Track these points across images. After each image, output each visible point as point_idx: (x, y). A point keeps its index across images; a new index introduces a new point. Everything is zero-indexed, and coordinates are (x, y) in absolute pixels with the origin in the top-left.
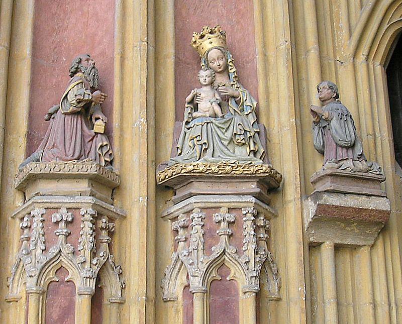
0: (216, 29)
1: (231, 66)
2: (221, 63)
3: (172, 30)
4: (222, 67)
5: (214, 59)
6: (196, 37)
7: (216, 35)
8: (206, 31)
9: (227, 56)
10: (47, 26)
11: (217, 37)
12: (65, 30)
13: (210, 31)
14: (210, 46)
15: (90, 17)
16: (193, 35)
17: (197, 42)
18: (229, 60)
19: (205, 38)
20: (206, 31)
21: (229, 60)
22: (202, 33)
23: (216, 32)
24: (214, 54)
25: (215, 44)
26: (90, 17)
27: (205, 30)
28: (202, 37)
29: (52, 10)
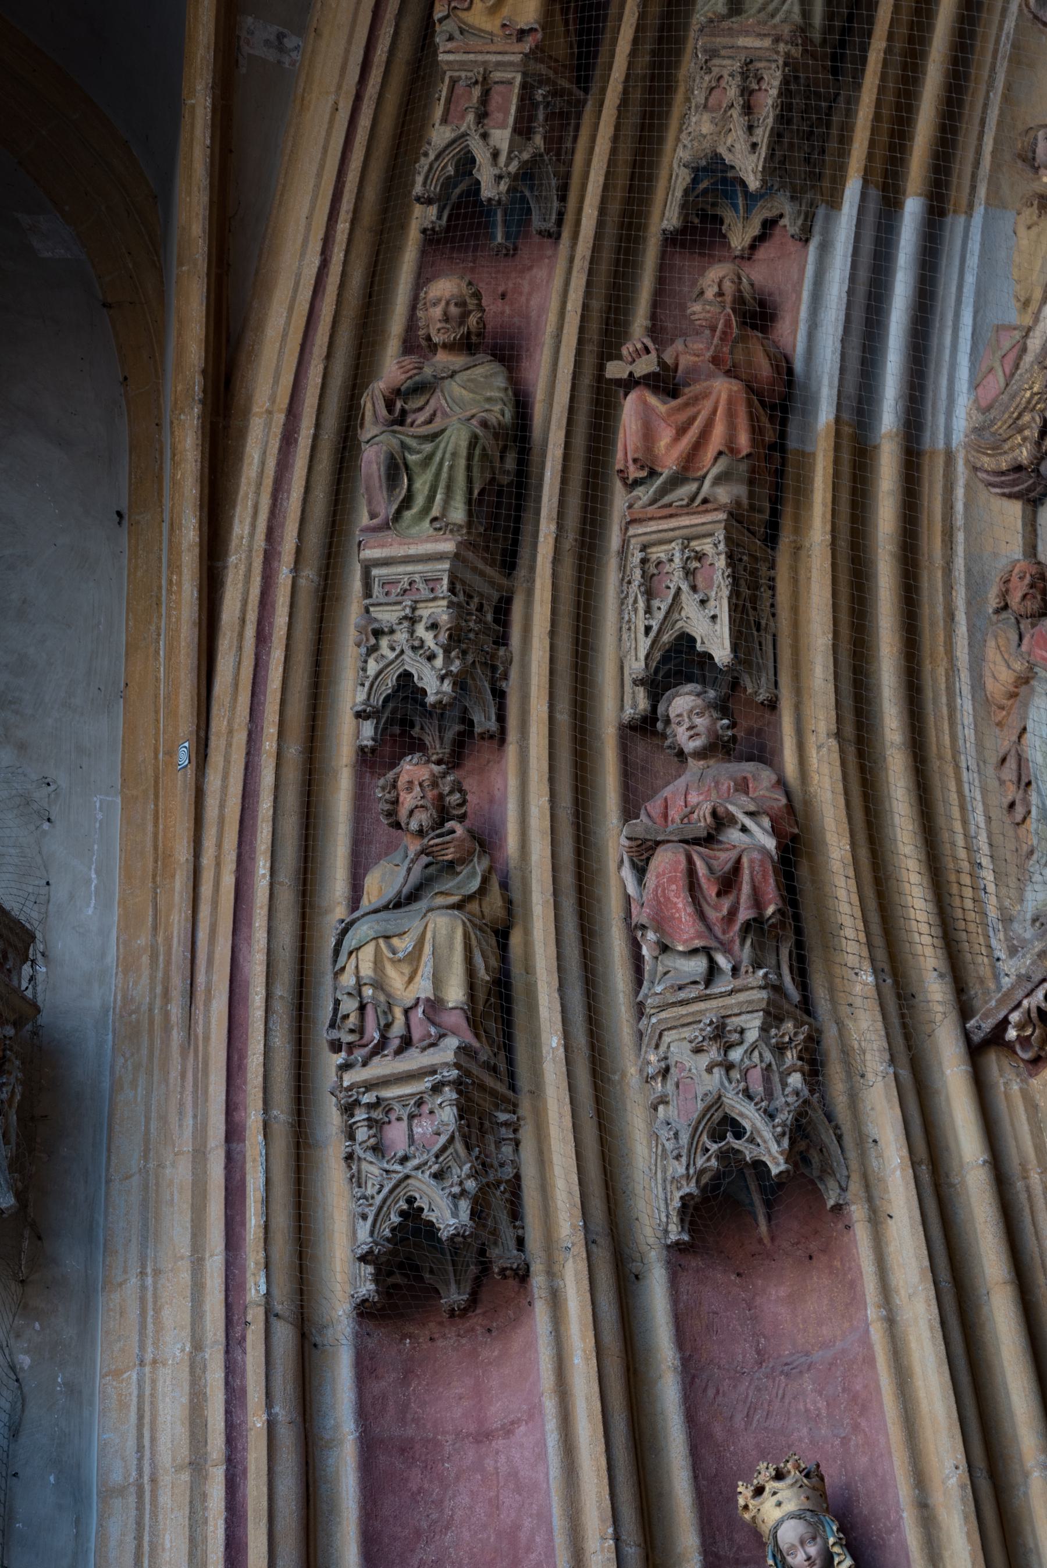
0: (789, 1466)
1: (839, 1555)
2: (813, 1550)
3: (686, 1486)
4: (817, 1562)
5: (793, 1546)
6: (744, 1492)
7: (789, 1481)
8: (764, 1473)
9: (824, 1531)
10: (400, 1529)
11: (792, 1485)
12: (447, 1528)
13: (773, 1473)
14: (777, 1514)
15: (502, 1484)
16: (739, 1490)
17: (751, 1507)
18: (831, 1540)
19: (766, 1494)
20: (764, 1473)
21: (831, 1540)
22: (755, 1482)
23: (789, 1472)
24: (790, 1533)
25: (791, 1506)
26: (502, 1484)
27: (763, 1473)
28: (759, 1491)
29: (410, 1485)
